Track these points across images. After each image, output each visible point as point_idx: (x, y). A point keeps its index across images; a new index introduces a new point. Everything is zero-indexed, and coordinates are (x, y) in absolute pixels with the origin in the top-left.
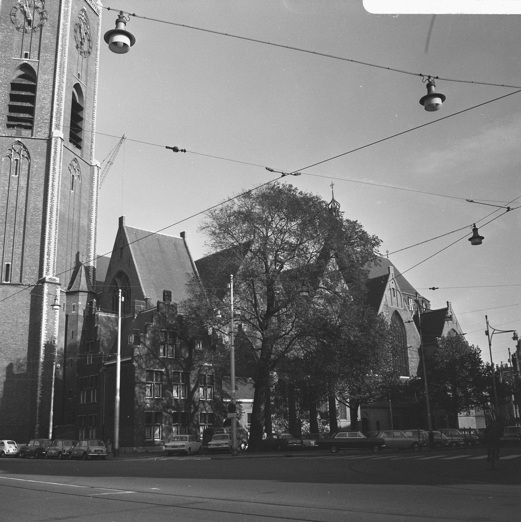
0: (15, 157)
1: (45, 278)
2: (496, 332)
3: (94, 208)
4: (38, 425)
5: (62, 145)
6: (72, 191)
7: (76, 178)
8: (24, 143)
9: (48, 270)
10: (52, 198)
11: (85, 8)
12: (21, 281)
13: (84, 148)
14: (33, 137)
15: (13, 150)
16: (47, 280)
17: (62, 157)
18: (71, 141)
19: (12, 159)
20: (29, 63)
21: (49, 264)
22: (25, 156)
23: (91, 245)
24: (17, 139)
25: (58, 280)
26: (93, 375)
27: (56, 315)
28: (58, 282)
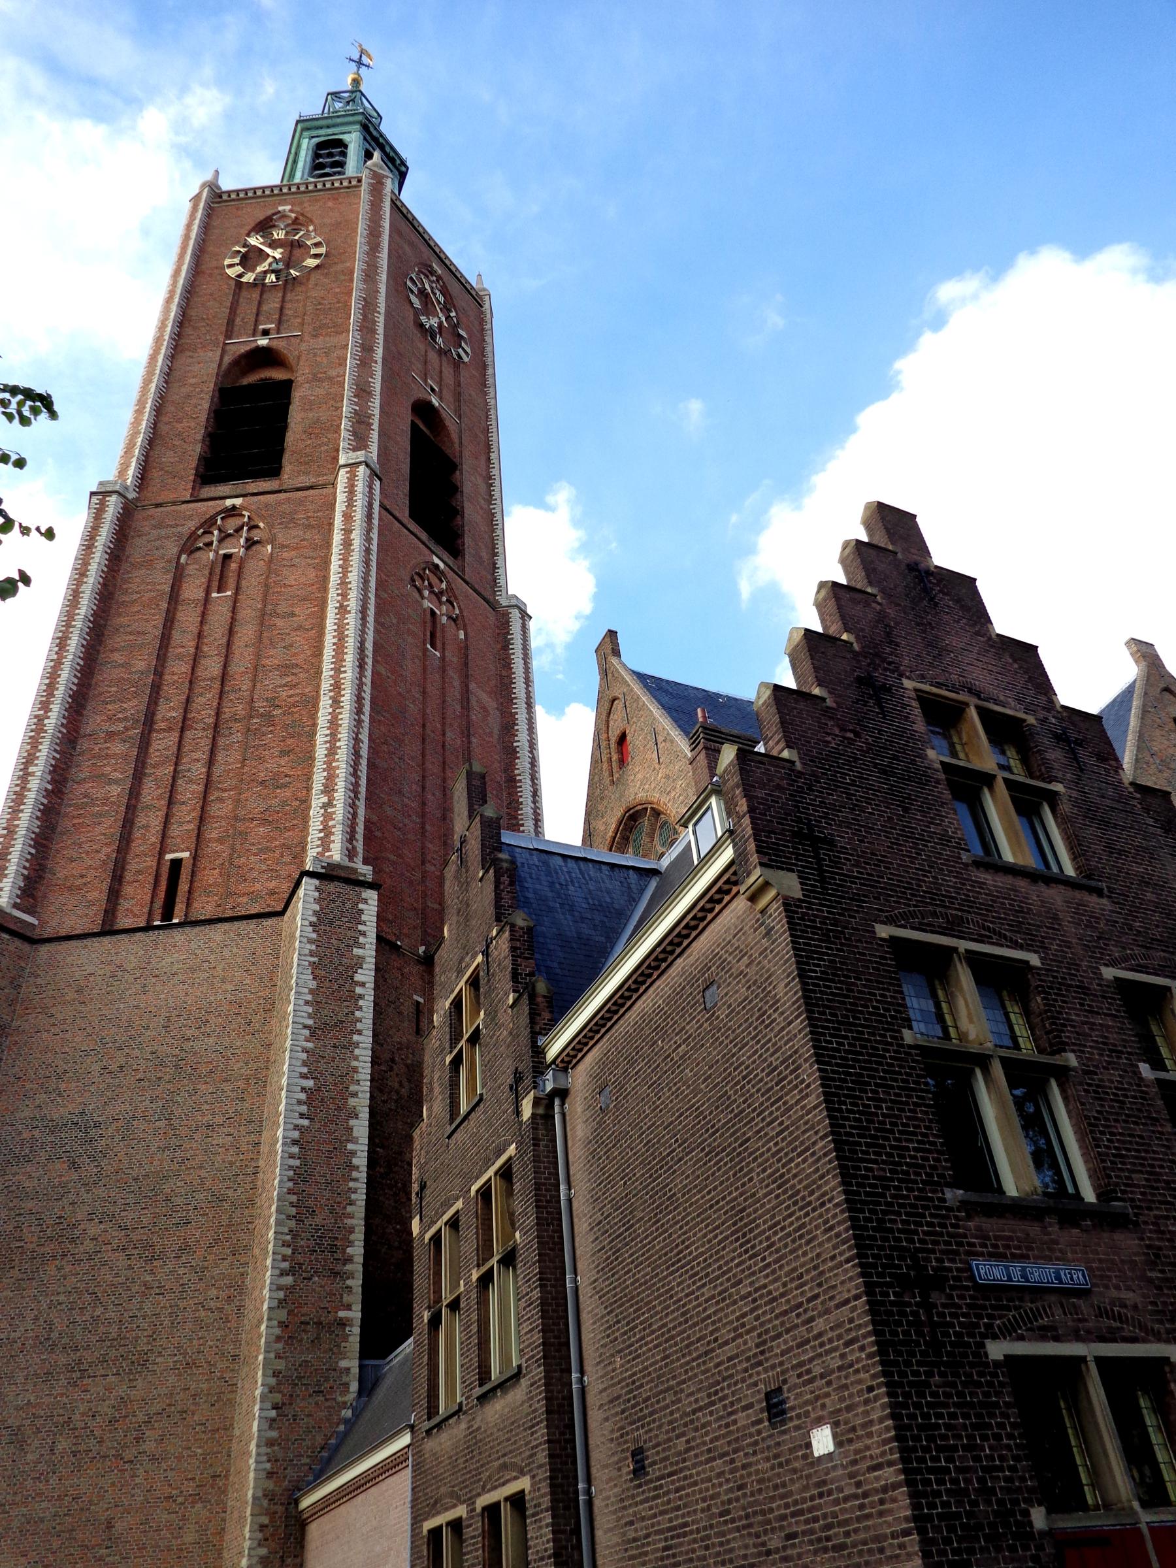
3: (522, 717)
10: (342, 618)
20: (275, 344)
21: (331, 823)
23: (522, 825)
24: (229, 503)
25: (366, 871)
27: (360, 1008)
28: (369, 878)
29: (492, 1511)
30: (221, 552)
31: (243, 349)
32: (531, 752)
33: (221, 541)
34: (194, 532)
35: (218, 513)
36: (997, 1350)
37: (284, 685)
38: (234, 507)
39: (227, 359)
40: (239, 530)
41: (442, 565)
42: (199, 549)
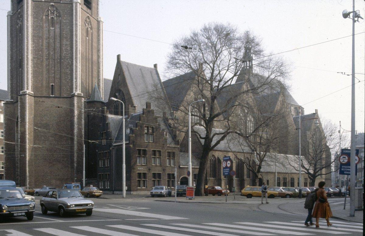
0: (52, 16)
1: (75, 93)
2: (345, 131)
4: (76, 178)
5: (80, 7)
6: (87, 38)
7: (89, 29)
8: (56, 6)
9: (76, 88)
12: (61, 95)
13: (93, 9)
14: (61, 2)
15: (49, 11)
16: (76, 94)
17: (80, 15)
18: (85, 4)
19: (50, 17)
22: (58, 15)
24: (51, 4)
26: (107, 151)
29: (106, 174)
30: (51, 17)
32: (102, 57)
33: (51, 14)
36: (137, 172)
38: (52, 5)
40: (54, 11)
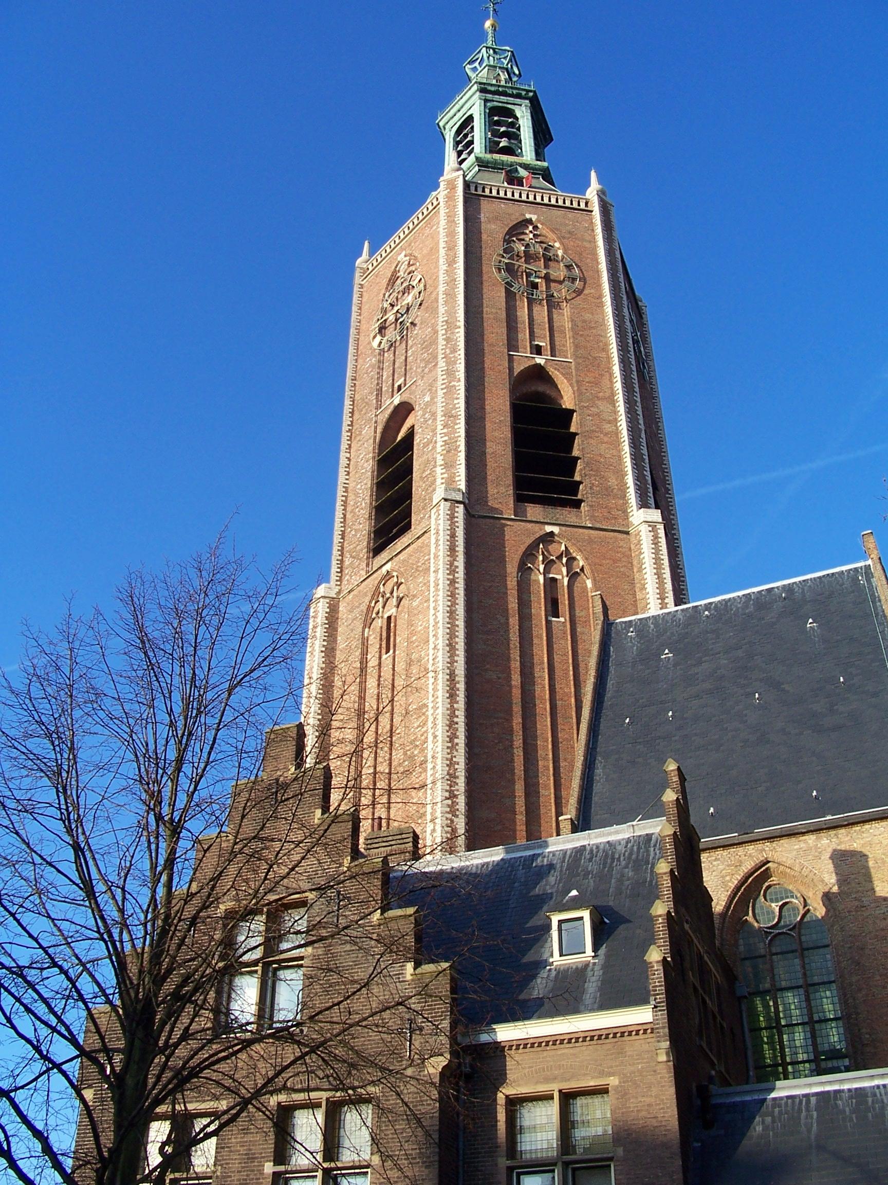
11: (528, 216)
24: (384, 570)
30: (386, 616)
31: (389, 411)
34: (369, 606)
35: (380, 583)
37: (419, 726)
39: (379, 429)
40: (392, 593)
41: (556, 529)
42: (374, 619)
